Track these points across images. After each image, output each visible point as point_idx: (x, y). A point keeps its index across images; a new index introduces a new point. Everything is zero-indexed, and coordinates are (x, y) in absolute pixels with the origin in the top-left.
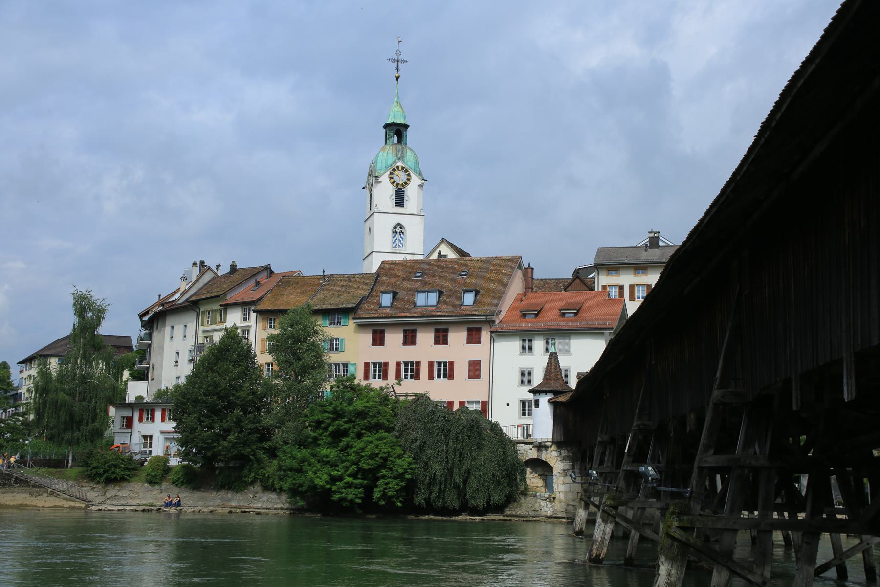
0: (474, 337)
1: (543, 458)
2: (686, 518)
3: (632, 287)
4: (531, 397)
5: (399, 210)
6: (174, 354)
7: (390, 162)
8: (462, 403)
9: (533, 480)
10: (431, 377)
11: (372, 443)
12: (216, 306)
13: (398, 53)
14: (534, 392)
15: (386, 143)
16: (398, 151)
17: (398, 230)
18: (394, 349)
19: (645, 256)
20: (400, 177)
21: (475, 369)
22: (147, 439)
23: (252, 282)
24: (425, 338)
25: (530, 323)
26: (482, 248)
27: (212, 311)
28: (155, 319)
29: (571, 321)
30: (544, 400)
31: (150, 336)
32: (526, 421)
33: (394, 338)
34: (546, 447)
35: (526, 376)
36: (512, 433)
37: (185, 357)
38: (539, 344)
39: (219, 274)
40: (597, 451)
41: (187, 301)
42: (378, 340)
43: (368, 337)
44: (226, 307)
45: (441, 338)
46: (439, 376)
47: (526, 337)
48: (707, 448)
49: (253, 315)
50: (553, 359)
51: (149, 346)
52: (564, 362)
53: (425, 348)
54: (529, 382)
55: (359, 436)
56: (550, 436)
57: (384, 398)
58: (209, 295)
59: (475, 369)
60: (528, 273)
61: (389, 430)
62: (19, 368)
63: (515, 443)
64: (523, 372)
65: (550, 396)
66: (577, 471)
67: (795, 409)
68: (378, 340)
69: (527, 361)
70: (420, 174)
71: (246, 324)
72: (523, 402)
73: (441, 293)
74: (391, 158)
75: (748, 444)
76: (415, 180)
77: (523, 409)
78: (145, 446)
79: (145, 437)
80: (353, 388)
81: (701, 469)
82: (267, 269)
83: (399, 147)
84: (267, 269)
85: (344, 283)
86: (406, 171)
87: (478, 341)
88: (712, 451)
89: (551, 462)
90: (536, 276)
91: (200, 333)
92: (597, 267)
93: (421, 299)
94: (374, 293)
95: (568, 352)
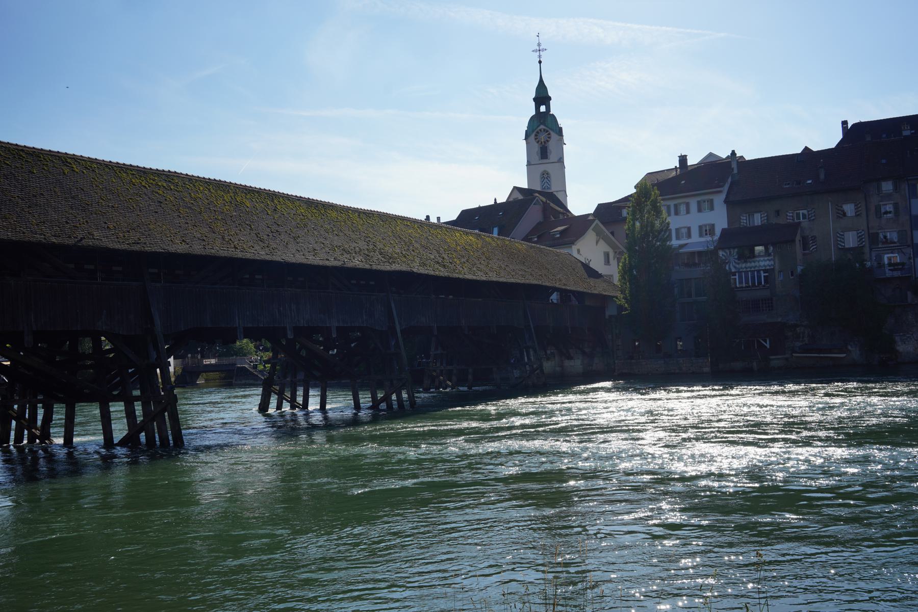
5: (545, 161)
13: (539, 45)
17: (546, 176)
20: (543, 137)
76: (553, 135)
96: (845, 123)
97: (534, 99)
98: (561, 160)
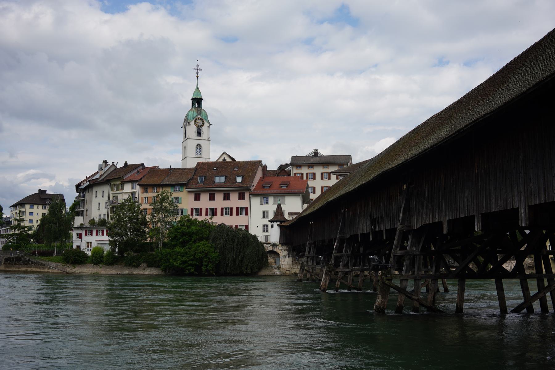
0: (242, 197)
1: (275, 250)
2: (389, 276)
3: (307, 174)
4: (270, 224)
6: (98, 204)
7: (195, 116)
8: (237, 226)
9: (271, 260)
10: (222, 214)
11: (203, 245)
12: (119, 183)
13: (198, 66)
14: (271, 221)
16: (198, 111)
17: (199, 147)
18: (205, 203)
19: (312, 160)
20: (199, 122)
22: (89, 244)
23: (136, 171)
24: (219, 197)
25: (267, 190)
26: (241, 156)
27: (117, 185)
28: (85, 188)
29: (285, 189)
30: (275, 224)
31: (84, 196)
32: (266, 234)
33: (205, 197)
34: (276, 245)
35: (265, 214)
36: (261, 240)
37: (103, 206)
38: (271, 199)
39: (118, 167)
40: (307, 246)
41: (103, 179)
42: (197, 198)
43: (192, 196)
44: (124, 182)
45: (227, 197)
46: (226, 214)
47: (264, 196)
48: (397, 247)
49: (137, 187)
50: (279, 206)
51: (83, 200)
52: (283, 207)
53: (219, 202)
54: (267, 217)
55: (195, 242)
56: (278, 241)
57: (205, 224)
58: (116, 177)
60: (265, 167)
61: (207, 239)
62: (10, 209)
63: (262, 244)
64: (264, 212)
65: (278, 223)
67: (445, 233)
68: (197, 198)
69: (265, 207)
70: (208, 121)
72: (264, 226)
73: (226, 177)
74: (195, 114)
75: (412, 245)
76: (206, 123)
77: (264, 229)
78: (88, 247)
79: (88, 243)
80: (189, 220)
81: (394, 256)
82: (143, 165)
83: (199, 109)
84: (143, 165)
87: (243, 198)
88: (398, 249)
89: (279, 252)
90: (268, 169)
91: (111, 195)
92: (291, 164)
93: (217, 180)
94: (195, 176)
95: (284, 204)
97: (192, 100)
98: (209, 140)
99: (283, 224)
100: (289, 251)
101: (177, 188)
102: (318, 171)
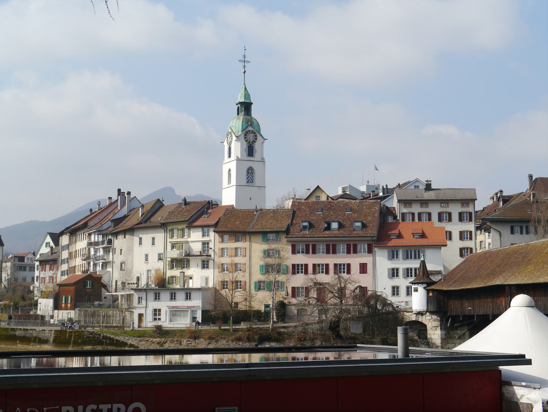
1: (420, 320)
7: (244, 127)
13: (244, 56)
15: (238, 114)
20: (251, 137)
21: (363, 268)
49: (212, 234)
50: (423, 263)
58: (176, 220)
59: (363, 268)
65: (425, 285)
66: (443, 327)
71: (206, 239)
72: (393, 288)
79: (155, 310)
85: (271, 215)
86: (255, 133)
96: (531, 177)
98: (263, 161)
99: (433, 287)
100: (441, 321)
101: (271, 236)
102: (435, 210)
